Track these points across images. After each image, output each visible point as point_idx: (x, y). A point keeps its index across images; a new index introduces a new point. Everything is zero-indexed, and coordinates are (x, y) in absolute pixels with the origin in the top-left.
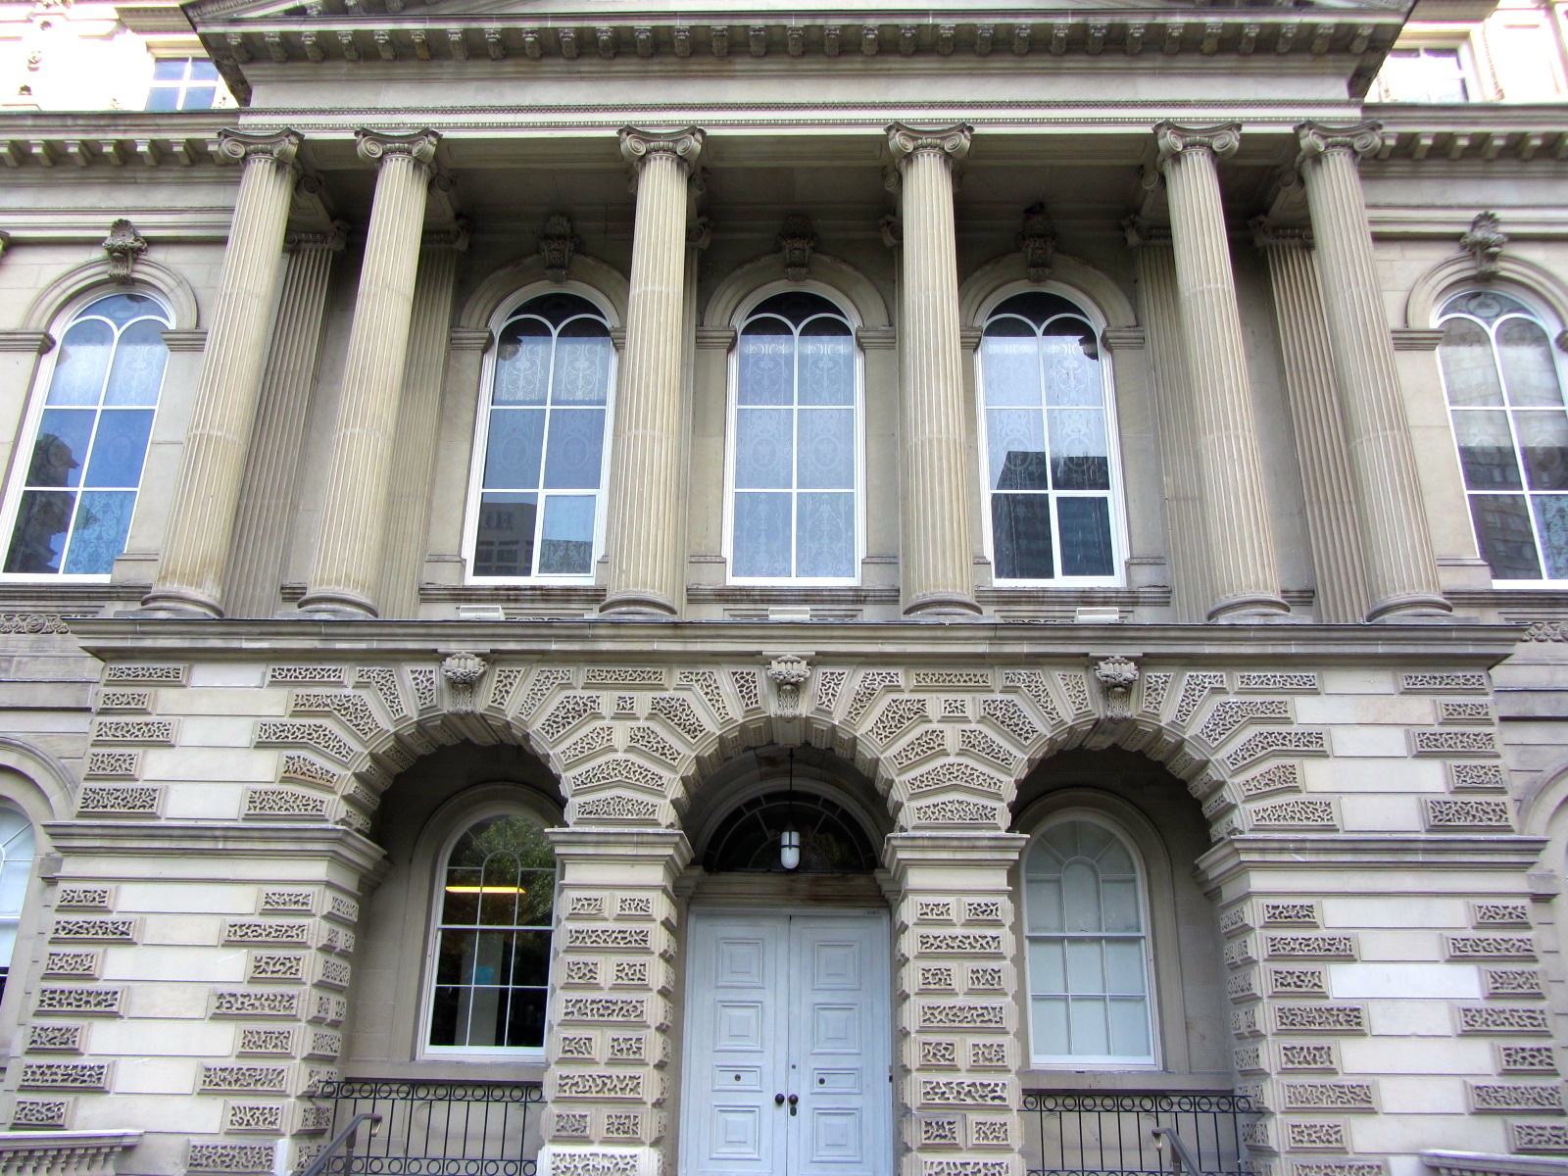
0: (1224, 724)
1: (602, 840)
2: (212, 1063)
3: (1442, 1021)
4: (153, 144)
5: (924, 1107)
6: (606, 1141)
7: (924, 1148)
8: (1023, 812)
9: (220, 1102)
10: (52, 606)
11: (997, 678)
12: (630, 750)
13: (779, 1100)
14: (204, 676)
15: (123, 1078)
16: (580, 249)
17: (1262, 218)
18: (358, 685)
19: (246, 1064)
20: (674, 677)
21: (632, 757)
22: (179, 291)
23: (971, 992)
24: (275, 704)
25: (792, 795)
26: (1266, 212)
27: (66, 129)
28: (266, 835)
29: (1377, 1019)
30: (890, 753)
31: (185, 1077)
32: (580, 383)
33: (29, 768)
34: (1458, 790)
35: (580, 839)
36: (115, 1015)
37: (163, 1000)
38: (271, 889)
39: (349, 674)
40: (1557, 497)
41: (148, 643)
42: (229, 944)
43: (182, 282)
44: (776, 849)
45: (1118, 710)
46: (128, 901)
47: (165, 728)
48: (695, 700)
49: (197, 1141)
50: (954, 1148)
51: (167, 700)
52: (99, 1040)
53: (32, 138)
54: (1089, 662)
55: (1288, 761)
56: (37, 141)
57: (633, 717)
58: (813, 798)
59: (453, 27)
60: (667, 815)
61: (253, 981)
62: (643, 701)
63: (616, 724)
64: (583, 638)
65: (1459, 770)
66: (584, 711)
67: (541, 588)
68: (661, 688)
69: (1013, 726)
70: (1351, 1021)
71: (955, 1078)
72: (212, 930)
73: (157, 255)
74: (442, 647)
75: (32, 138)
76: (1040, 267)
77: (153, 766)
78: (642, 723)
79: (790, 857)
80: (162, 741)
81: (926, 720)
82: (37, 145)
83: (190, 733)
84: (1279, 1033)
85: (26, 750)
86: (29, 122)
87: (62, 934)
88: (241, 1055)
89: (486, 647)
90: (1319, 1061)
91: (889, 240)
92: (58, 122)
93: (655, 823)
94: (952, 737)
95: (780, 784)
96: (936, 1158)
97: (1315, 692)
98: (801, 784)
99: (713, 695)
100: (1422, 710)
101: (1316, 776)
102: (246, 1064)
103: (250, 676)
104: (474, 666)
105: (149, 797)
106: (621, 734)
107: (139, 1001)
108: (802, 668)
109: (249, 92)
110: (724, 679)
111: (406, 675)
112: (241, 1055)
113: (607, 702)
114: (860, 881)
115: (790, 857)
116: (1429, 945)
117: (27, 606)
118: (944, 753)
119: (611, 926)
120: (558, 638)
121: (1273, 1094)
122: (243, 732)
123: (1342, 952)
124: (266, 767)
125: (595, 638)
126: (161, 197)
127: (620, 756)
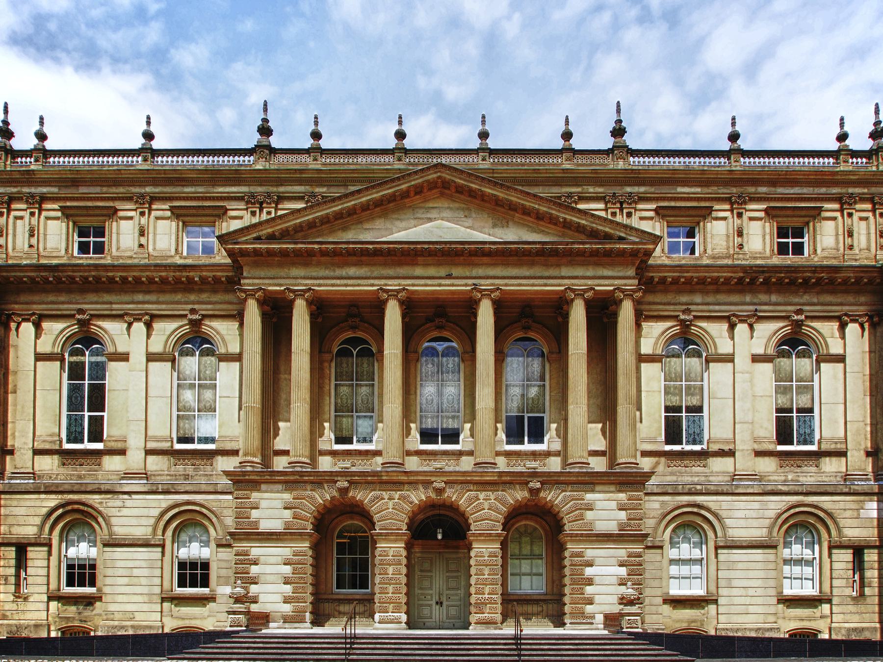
1: (387, 535)
4: (200, 277)
5: (475, 603)
7: (475, 613)
8: (506, 526)
13: (437, 603)
16: (363, 320)
17: (606, 311)
21: (394, 511)
25: (440, 515)
26: (607, 309)
32: (365, 373)
35: (381, 534)
37: (269, 578)
40: (694, 416)
44: (436, 533)
49: (284, 614)
50: (483, 613)
53: (155, 274)
58: (448, 516)
60: (405, 527)
62: (397, 495)
67: (358, 450)
69: (503, 502)
71: (484, 596)
73: (207, 322)
76: (526, 328)
78: (396, 501)
79: (440, 537)
91: (473, 320)
93: (402, 530)
95: (437, 512)
96: (478, 615)
98: (442, 512)
105: (256, 523)
107: (262, 579)
109: (242, 268)
114: (461, 543)
115: (440, 537)
116: (614, 561)
119: (390, 557)
127: (390, 510)
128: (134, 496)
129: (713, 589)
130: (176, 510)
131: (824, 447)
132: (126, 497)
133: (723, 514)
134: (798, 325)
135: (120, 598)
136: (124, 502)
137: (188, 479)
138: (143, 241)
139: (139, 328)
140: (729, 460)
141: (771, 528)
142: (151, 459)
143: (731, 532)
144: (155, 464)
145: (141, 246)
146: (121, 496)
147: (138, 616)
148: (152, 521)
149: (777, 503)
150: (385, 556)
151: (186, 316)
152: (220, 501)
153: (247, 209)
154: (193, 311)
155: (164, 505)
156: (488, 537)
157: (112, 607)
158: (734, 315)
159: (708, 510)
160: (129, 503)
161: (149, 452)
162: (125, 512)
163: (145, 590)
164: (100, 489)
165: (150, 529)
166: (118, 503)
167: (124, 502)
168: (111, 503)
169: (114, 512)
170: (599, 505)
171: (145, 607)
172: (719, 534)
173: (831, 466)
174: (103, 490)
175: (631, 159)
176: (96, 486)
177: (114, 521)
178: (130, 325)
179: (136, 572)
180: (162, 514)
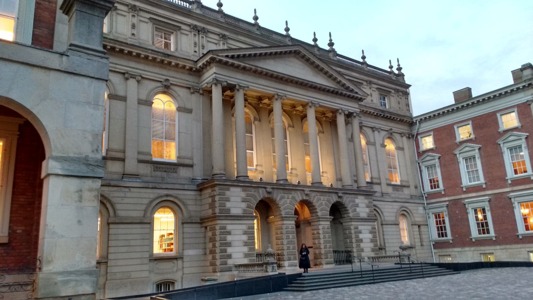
0: (349, 202)
2: (245, 253)
3: (369, 240)
6: (293, 260)
9: (247, 258)
10: (169, 166)
11: (328, 194)
12: (289, 203)
14: (232, 189)
15: (234, 256)
18: (254, 192)
19: (250, 252)
20: (293, 192)
22: (179, 98)
23: (328, 238)
24: (243, 195)
27: (158, 55)
28: (247, 217)
29: (364, 241)
30: (318, 205)
31: (241, 255)
33: (176, 201)
34: (370, 212)
36: (231, 246)
38: (249, 225)
39: (253, 190)
41: (226, 183)
42: (244, 234)
43: (179, 96)
45: (340, 200)
46: (229, 227)
47: (228, 198)
48: (296, 195)
51: (228, 193)
52: (229, 250)
54: (337, 193)
55: (355, 207)
56: (151, 56)
57: (289, 198)
59: (254, 67)
61: (249, 240)
62: (290, 196)
63: (287, 199)
64: (284, 186)
65: (370, 209)
66: (283, 198)
68: (292, 194)
70: (361, 241)
72: (241, 232)
73: (172, 87)
74: (267, 186)
75: (150, 55)
77: (228, 205)
80: (228, 200)
81: (320, 200)
82: (143, 55)
83: (232, 199)
84: (356, 242)
85: (176, 198)
86: (150, 51)
87: (221, 233)
88: (249, 251)
89: (272, 187)
90: (358, 246)
92: (157, 53)
94: (324, 202)
97: (357, 198)
99: (298, 195)
100: (366, 201)
101: (358, 209)
102: (250, 252)
103: (238, 190)
104: (271, 190)
106: (288, 201)
108: (309, 192)
110: (299, 193)
111: (261, 190)
112: (249, 251)
113: (286, 196)
117: (164, 166)
118: (323, 205)
120: (282, 186)
121: (355, 250)
122: (239, 199)
123: (360, 232)
124: (244, 205)
125: (285, 186)
126: (172, 73)
128: (132, 190)
129: (383, 244)
130: (160, 200)
131: (404, 184)
132: (127, 190)
133: (383, 210)
134: (391, 134)
135: (120, 263)
136: (125, 194)
137: (164, 180)
138: (134, 32)
139: (132, 82)
140: (379, 186)
141: (396, 217)
142: (142, 165)
143: (387, 219)
144: (145, 170)
145: (133, 34)
146: (123, 189)
147: (134, 275)
148: (144, 207)
149: (397, 206)
150: (288, 229)
151: (161, 82)
152: (185, 195)
153: (191, 32)
154: (167, 80)
155: (152, 196)
156: (325, 219)
157: (115, 270)
158: (375, 127)
159: (379, 208)
160: (129, 195)
161: (140, 161)
162: (126, 200)
163: (139, 255)
164: (110, 184)
165: (143, 213)
166: (122, 194)
167: (125, 194)
168: (116, 194)
169: (118, 200)
170: (360, 205)
171: (139, 268)
172: (382, 219)
173: (406, 191)
174: (112, 185)
175: (337, 57)
176: (108, 182)
177: (118, 207)
178: (127, 79)
179: (133, 243)
180: (151, 202)
